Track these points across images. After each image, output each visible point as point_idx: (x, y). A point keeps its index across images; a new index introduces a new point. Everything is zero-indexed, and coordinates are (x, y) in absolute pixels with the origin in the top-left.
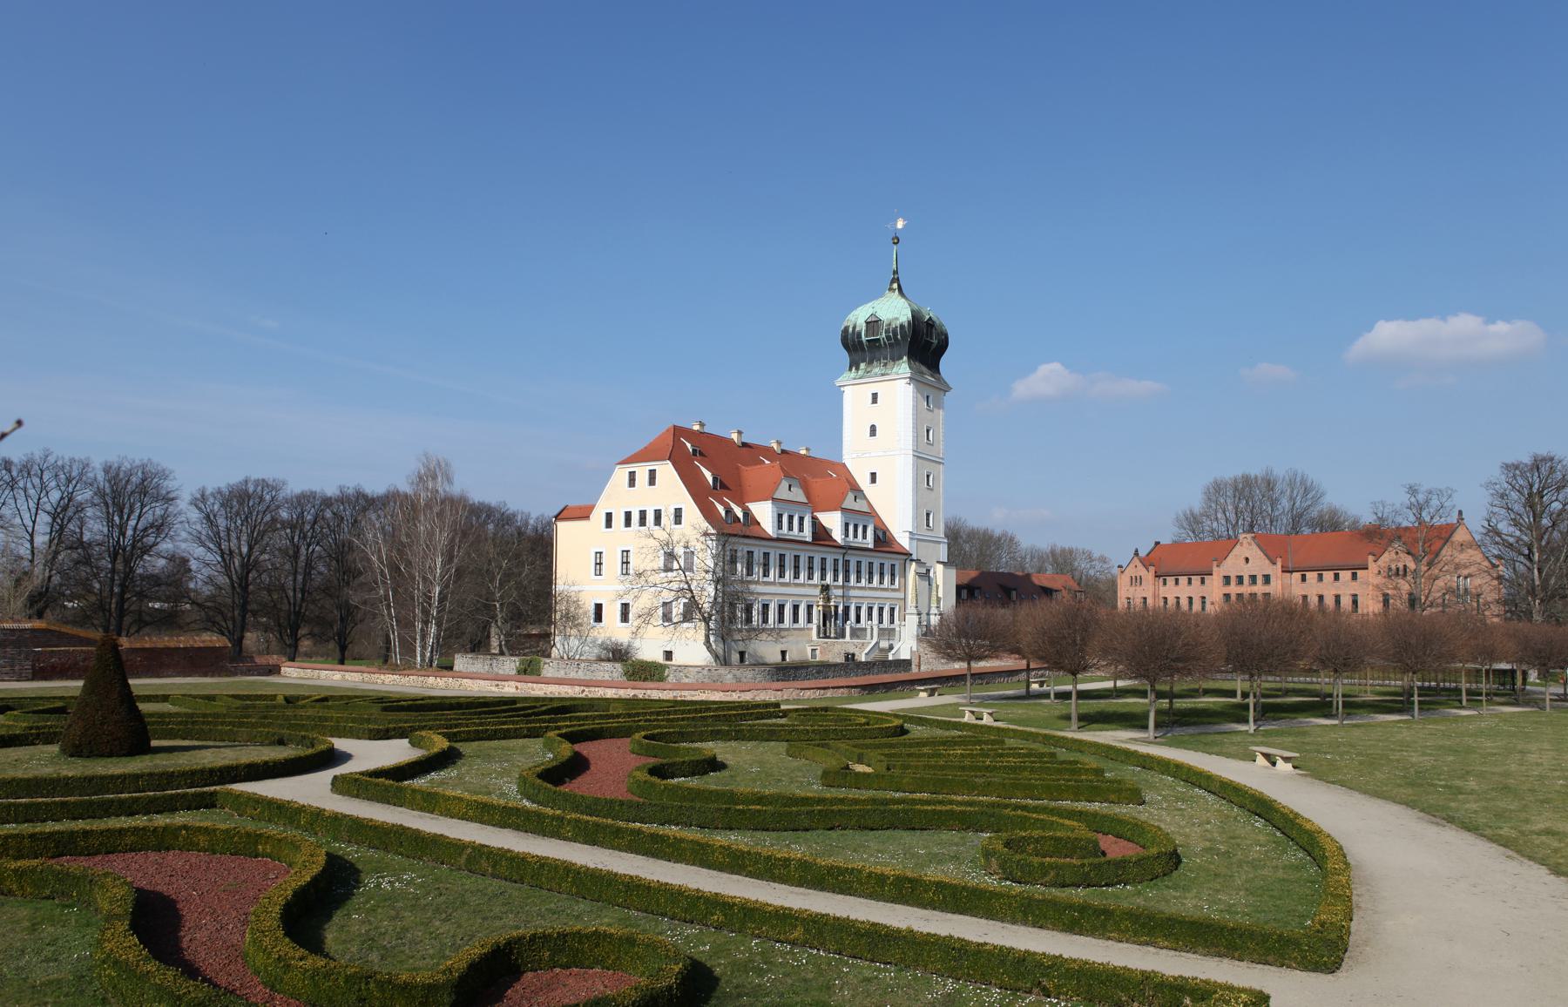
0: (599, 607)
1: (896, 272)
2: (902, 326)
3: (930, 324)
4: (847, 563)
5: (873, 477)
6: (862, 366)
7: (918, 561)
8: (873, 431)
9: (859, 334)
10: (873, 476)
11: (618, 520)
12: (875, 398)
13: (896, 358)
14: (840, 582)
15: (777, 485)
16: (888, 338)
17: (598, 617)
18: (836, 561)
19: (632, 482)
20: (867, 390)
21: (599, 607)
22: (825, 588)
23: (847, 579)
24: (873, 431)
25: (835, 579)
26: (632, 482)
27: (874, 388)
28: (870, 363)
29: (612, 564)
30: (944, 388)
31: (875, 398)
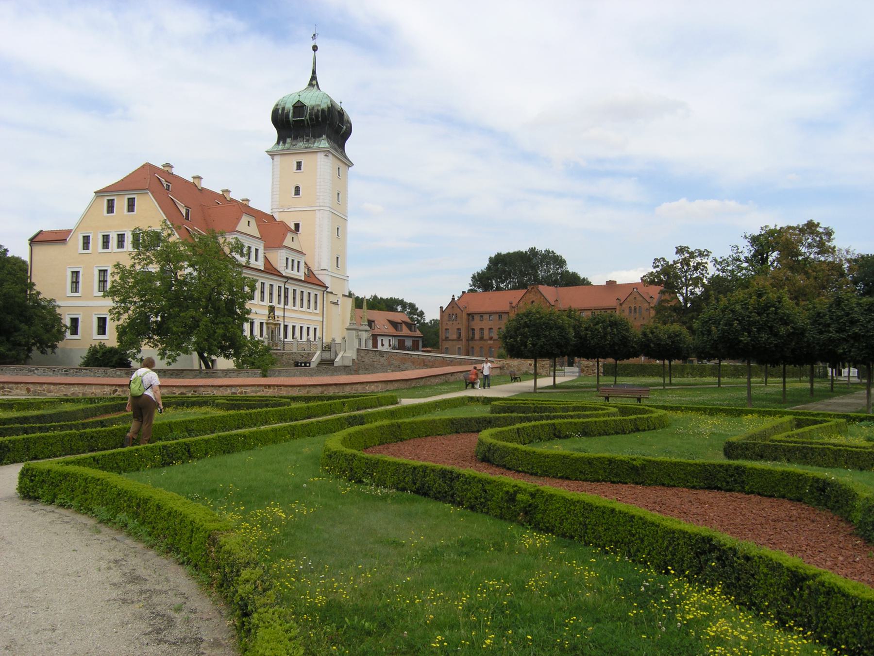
0: (75, 321)
1: (314, 72)
2: (323, 110)
3: (341, 114)
4: (286, 289)
5: (297, 226)
6: (289, 140)
7: (331, 293)
8: (297, 190)
9: (288, 115)
10: (297, 226)
11: (96, 242)
12: (299, 165)
13: (317, 136)
14: (282, 306)
15: (238, 219)
16: (311, 119)
17: (74, 329)
18: (280, 287)
19: (110, 208)
20: (293, 161)
21: (75, 321)
22: (272, 309)
23: (286, 303)
24: (297, 190)
25: (279, 303)
26: (110, 208)
27: (299, 158)
28: (295, 138)
29: (90, 281)
30: (349, 164)
31: (299, 165)
